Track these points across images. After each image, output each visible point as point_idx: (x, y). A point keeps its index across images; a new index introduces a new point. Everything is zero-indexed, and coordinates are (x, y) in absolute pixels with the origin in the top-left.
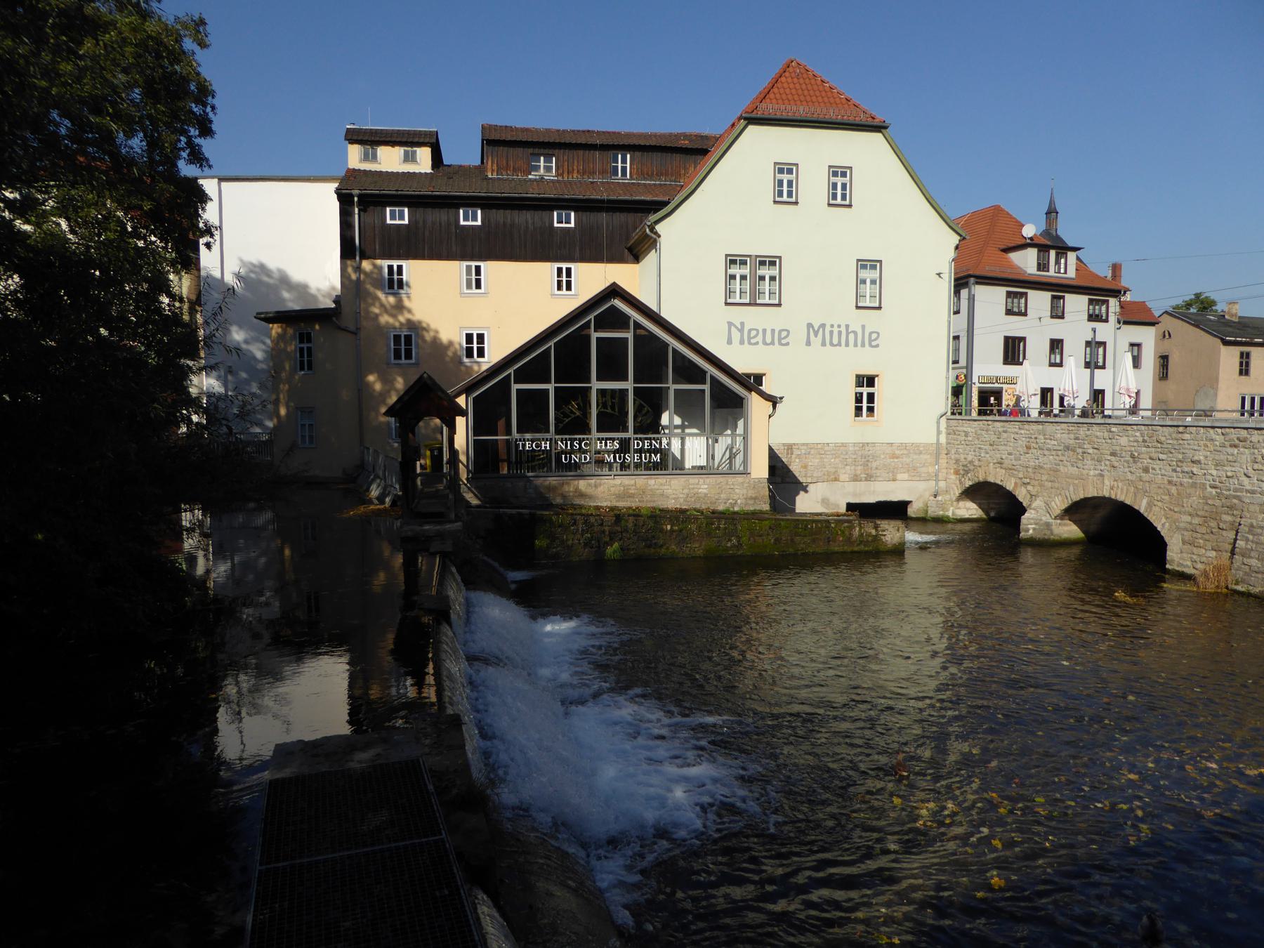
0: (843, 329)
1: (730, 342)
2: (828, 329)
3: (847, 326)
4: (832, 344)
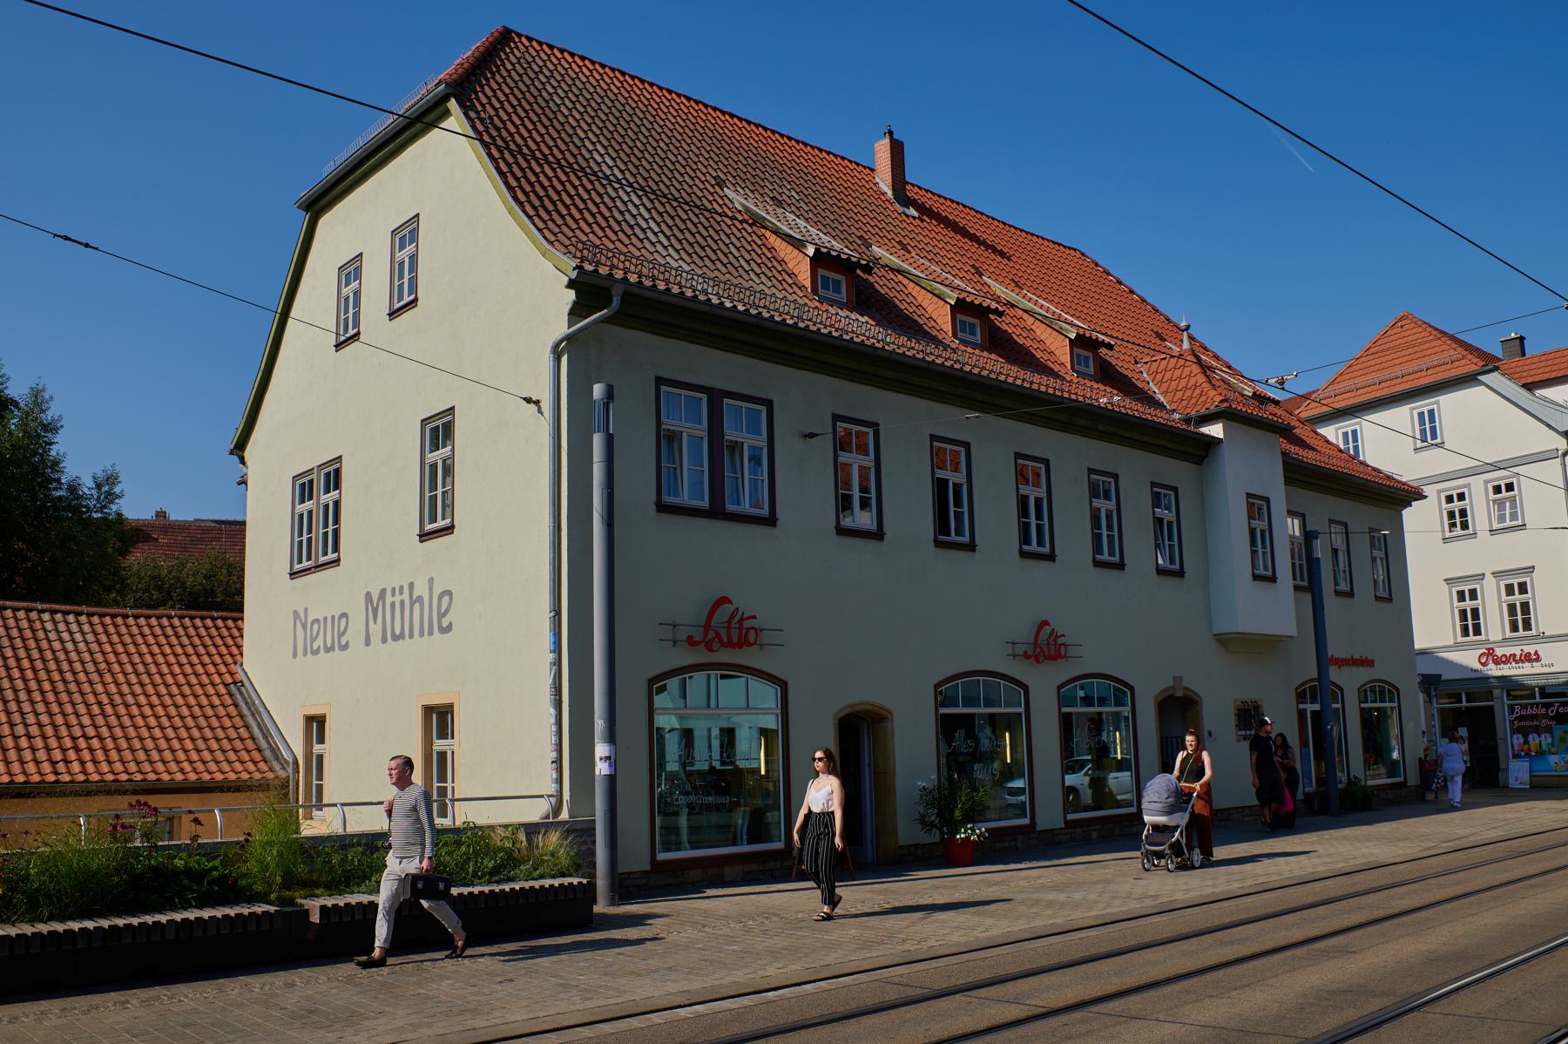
0: (406, 596)
1: (295, 655)
2: (389, 599)
3: (411, 585)
4: (396, 638)
